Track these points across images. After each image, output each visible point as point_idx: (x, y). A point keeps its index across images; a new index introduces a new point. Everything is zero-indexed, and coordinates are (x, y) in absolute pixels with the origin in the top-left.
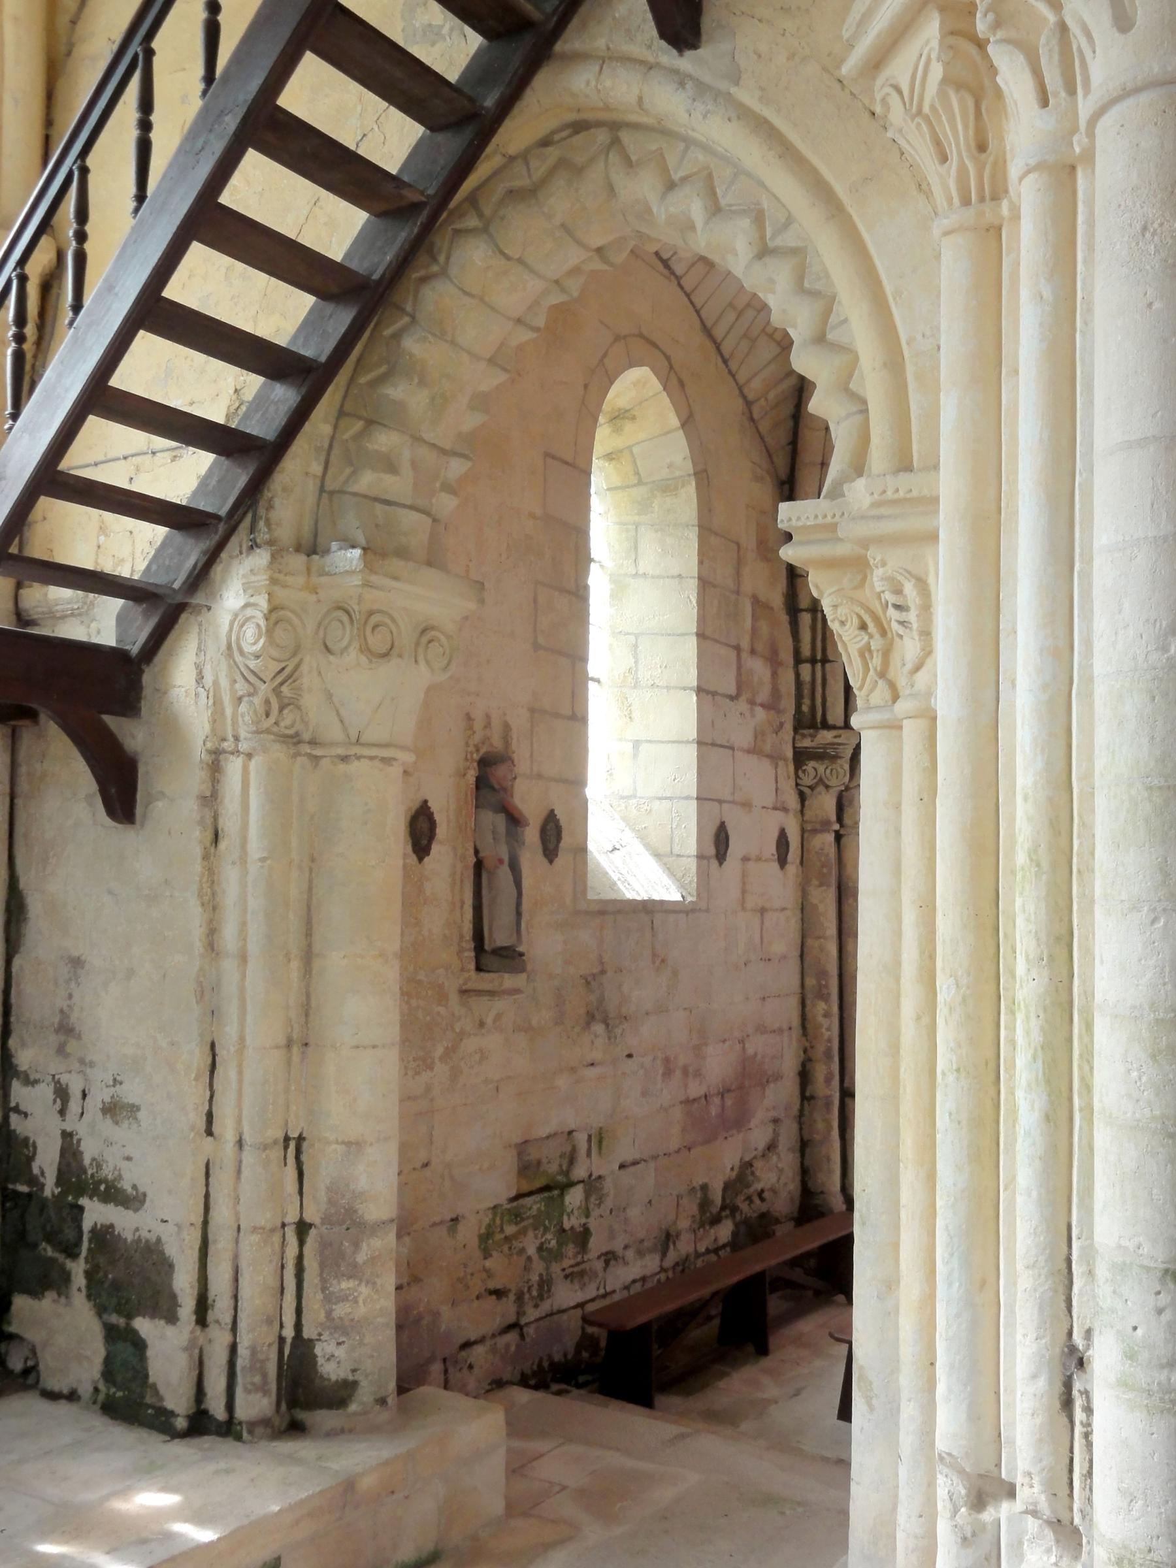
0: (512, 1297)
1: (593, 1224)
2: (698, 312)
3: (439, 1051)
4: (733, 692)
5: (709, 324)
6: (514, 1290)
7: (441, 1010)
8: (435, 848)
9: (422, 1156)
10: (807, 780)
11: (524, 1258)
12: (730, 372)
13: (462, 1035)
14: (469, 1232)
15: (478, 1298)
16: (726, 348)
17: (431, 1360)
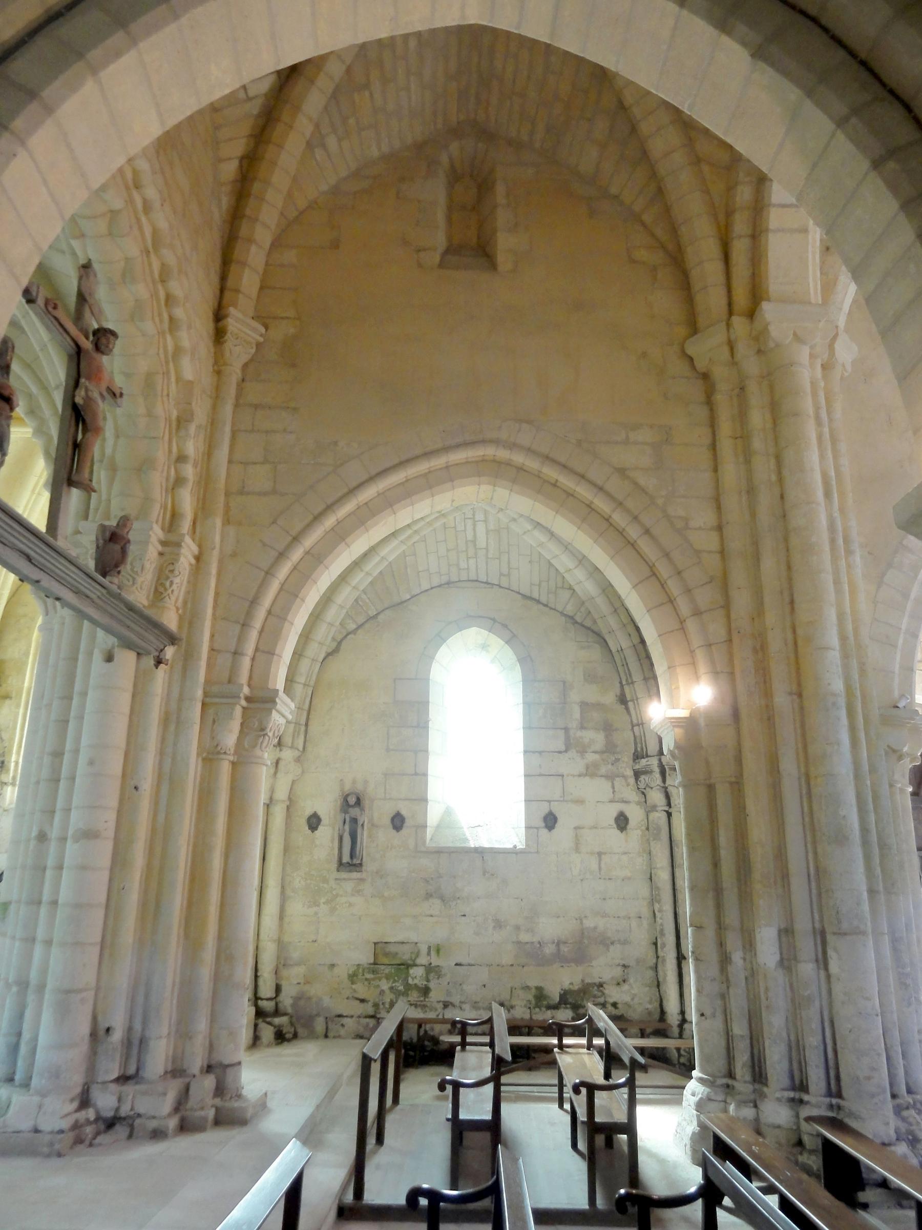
0: (370, 1004)
1: (432, 985)
2: (519, 593)
3: (323, 900)
4: (563, 748)
5: (528, 594)
6: (372, 1001)
7: (325, 886)
8: (320, 828)
9: (314, 938)
10: (642, 786)
11: (378, 991)
12: (551, 608)
13: (337, 896)
14: (342, 972)
15: (348, 998)
16: (544, 599)
17: (318, 1015)
